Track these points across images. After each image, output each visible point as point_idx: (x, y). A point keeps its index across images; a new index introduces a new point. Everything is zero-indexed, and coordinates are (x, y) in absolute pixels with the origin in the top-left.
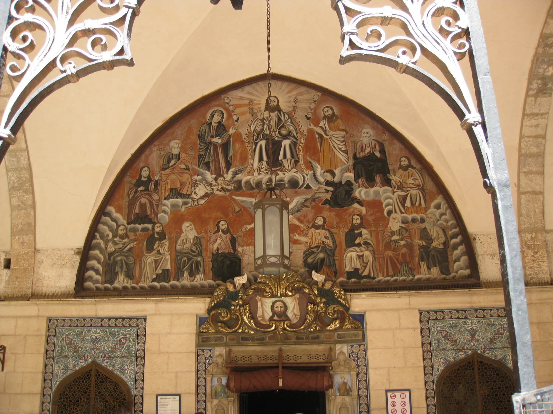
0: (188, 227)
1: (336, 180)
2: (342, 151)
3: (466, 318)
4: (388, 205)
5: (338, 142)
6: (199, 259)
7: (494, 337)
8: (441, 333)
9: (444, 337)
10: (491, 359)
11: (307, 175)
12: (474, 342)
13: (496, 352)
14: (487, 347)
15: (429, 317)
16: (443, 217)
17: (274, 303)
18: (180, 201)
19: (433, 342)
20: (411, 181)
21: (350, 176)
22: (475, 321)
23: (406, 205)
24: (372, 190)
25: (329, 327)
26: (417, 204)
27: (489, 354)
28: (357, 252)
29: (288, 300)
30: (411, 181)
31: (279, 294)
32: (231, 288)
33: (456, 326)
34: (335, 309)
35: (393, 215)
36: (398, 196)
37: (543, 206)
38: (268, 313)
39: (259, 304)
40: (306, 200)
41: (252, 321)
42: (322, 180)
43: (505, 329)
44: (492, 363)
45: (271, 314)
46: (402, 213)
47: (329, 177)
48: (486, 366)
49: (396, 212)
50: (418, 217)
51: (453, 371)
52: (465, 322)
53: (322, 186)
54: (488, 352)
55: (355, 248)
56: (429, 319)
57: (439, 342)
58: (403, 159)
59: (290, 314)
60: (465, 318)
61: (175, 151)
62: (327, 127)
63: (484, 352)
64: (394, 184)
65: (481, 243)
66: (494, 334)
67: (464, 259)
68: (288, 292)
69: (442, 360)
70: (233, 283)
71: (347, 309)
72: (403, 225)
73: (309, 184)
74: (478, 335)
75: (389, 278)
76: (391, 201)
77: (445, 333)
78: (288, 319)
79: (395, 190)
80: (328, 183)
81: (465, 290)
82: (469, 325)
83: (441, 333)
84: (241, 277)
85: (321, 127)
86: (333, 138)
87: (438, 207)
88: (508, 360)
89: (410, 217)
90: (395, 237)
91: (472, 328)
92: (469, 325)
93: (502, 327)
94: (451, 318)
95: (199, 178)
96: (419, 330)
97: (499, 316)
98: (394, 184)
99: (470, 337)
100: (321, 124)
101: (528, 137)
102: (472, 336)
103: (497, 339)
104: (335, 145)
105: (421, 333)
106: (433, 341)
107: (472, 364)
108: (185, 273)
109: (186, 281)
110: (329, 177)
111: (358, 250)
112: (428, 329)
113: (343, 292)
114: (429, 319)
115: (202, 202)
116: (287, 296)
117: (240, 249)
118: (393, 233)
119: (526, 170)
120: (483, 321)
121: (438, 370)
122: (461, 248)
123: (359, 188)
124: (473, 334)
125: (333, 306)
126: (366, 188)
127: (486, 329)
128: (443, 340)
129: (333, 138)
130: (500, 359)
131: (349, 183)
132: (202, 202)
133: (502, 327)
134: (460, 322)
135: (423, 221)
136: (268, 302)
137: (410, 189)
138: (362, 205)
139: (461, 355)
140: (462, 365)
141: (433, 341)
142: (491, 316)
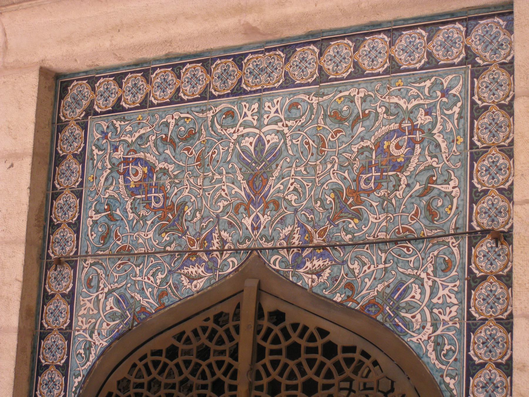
7: (357, 180)
8: (126, 173)
10: (328, 303)
12: (256, 211)
13: (356, 266)
14: (317, 240)
15: (92, 102)
27: (319, 274)
33: (191, 135)
43: (418, 136)
44: (325, 325)
48: (295, 337)
51: (150, 359)
52: (230, 113)
54: (318, 263)
56: (90, 111)
57: (111, 217)
60: (233, 93)
63: (298, 263)
66: (357, 165)
69: (111, 300)
82: (245, 125)
88: (410, 308)
93: (406, 125)
94: (176, 99)
102: (251, 182)
103: (368, 192)
106: (91, 213)
107: (231, 325)
114: (90, 111)
121: (88, 349)
127: (322, 142)
128: (128, 206)
130: (372, 303)
134: (210, 114)
139: (191, 279)
140: (188, 327)
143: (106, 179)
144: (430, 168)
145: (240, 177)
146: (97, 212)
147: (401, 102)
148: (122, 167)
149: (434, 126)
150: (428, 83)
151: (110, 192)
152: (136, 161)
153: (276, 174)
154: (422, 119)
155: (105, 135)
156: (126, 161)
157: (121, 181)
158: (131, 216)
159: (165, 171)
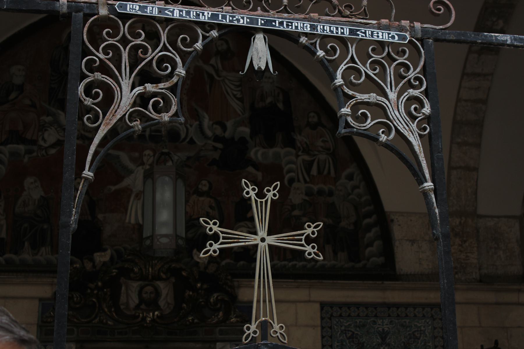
0: (32, 183)
1: (227, 134)
2: (238, 99)
3: (376, 316)
4: (289, 171)
5: (232, 87)
6: (45, 226)
8: (346, 333)
9: (348, 338)
11: (191, 126)
16: (357, 191)
17: (142, 288)
18: (21, 148)
19: (336, 344)
20: (319, 143)
21: (245, 130)
22: (386, 321)
23: (312, 173)
24: (271, 152)
25: (210, 320)
26: (326, 172)
28: (249, 227)
29: (161, 285)
30: (319, 143)
31: (150, 277)
32: (88, 266)
34: (219, 298)
35: (295, 185)
36: (304, 161)
37: (477, 185)
38: (134, 300)
39: (123, 288)
40: (189, 158)
41: (113, 309)
42: (209, 133)
43: (422, 332)
45: (137, 301)
46: (306, 182)
47: (219, 131)
49: (299, 181)
50: (326, 188)
52: (374, 321)
53: (210, 142)
55: (247, 222)
58: (312, 114)
59: (162, 303)
61: (18, 80)
62: (220, 65)
64: (299, 145)
65: (399, 225)
67: (378, 243)
68: (162, 274)
70: (92, 260)
71: (234, 298)
72: (307, 198)
73: (194, 138)
74: (390, 338)
75: (286, 263)
76: (293, 166)
77: (350, 333)
78: (158, 308)
79: (300, 153)
80: (217, 139)
81: (378, 282)
82: (379, 325)
83: (346, 333)
84: (103, 254)
85: (213, 66)
86: (227, 81)
87: (350, 178)
89: (315, 188)
90: (296, 213)
91: (383, 330)
92: (379, 325)
94: (358, 316)
95: (49, 119)
96: (319, 329)
97: (415, 316)
98: (299, 145)
99: (380, 341)
100: (213, 61)
101: (466, 101)
104: (229, 90)
105: (322, 332)
106: (336, 343)
108: (26, 244)
109: (27, 256)
110: (219, 131)
111: (250, 226)
112: (331, 328)
113: (229, 277)
115: (53, 151)
116: (160, 279)
117: (100, 216)
118: (294, 207)
119: (459, 140)
120: (397, 321)
122: (375, 230)
123: (255, 146)
124: (384, 336)
125: (215, 295)
126: (264, 147)
129: (227, 81)
131: (243, 140)
132: (53, 151)
133: (419, 329)
134: (369, 321)
135: (331, 194)
136: (135, 285)
137: (316, 153)
138: (257, 169)
141: (336, 343)
142: (407, 316)
143: (340, 334)
144: (425, 340)
145: (379, 337)
146: (338, 343)
147: (418, 324)
148: (344, 332)
149: (425, 330)
150: (423, 321)
151: (341, 338)
152: (349, 331)
153: (388, 337)
154: (423, 328)
155: (337, 322)
156: (345, 330)
157: (344, 335)
158: (348, 345)
159: (357, 334)
